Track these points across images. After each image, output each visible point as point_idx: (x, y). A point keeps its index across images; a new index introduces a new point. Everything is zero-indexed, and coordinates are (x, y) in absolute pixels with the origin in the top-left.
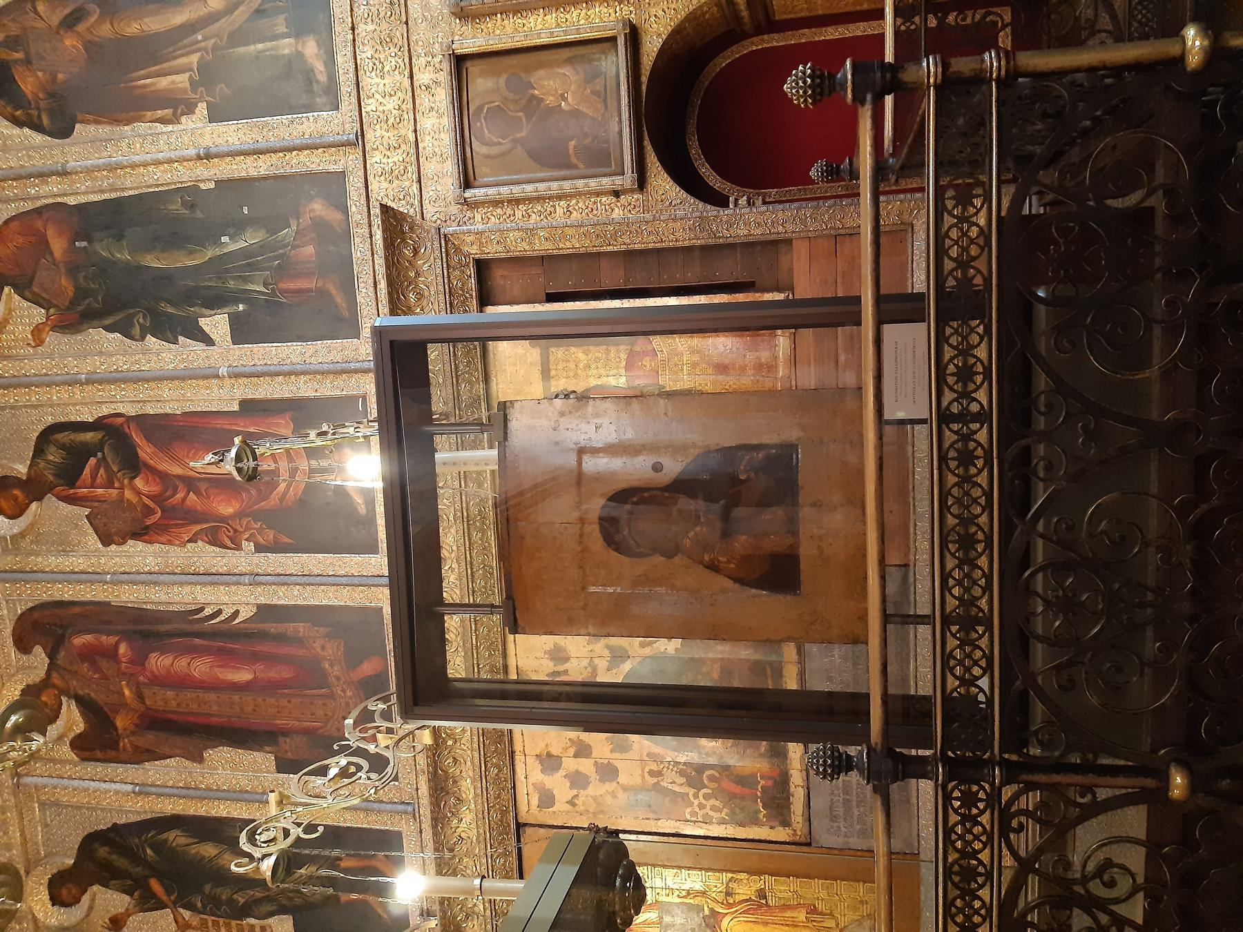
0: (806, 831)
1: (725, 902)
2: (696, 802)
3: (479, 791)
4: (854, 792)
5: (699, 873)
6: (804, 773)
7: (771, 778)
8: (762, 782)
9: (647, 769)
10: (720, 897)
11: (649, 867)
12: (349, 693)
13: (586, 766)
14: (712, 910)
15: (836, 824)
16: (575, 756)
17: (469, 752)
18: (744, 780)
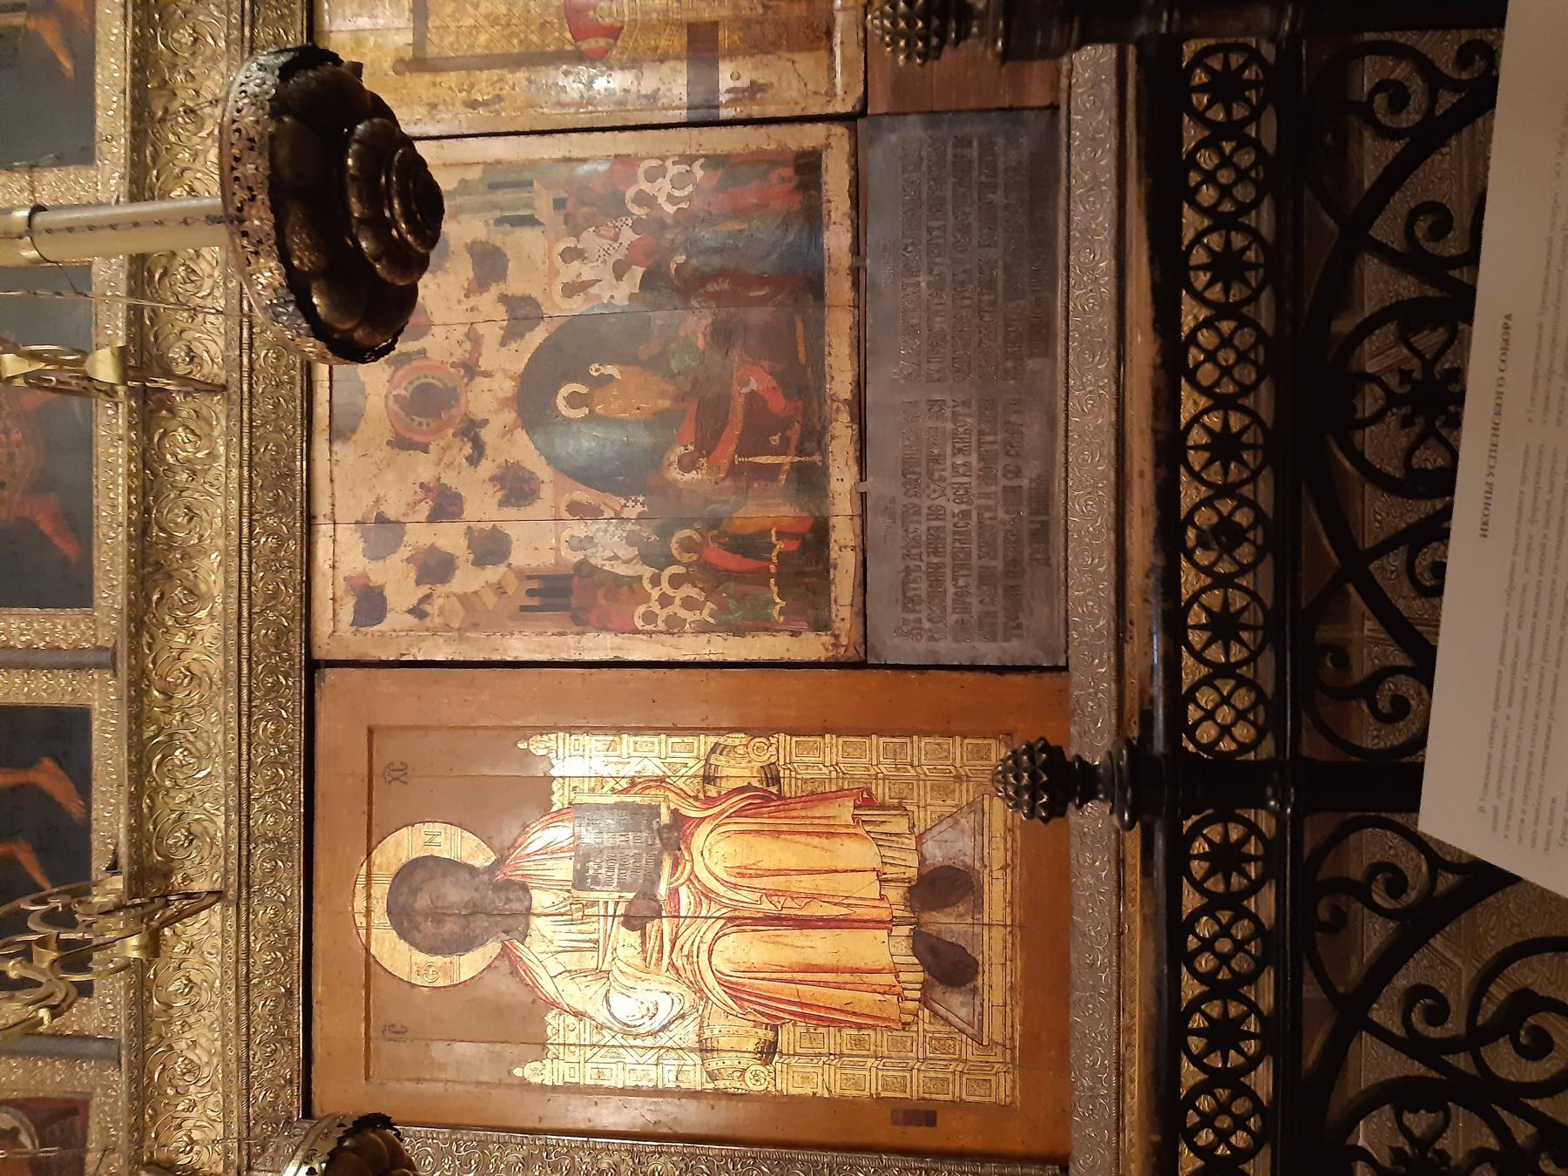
0: (857, 636)
1: (701, 796)
2: (655, 593)
3: (234, 577)
4: (949, 549)
5: (656, 739)
6: (858, 521)
8: (780, 546)
11: (561, 734)
12: (15, 436)
13: (450, 538)
14: (675, 813)
15: (911, 617)
16: (431, 519)
17: (220, 500)
18: (748, 545)
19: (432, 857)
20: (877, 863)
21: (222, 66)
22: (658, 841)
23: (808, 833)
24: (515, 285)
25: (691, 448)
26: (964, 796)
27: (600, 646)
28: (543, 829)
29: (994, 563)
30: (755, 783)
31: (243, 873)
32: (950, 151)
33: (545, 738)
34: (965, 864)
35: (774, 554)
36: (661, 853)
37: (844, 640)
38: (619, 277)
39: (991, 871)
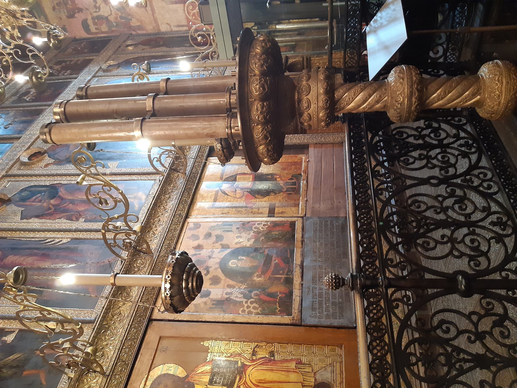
0: (299, 317)
2: (246, 305)
6: (301, 290)
7: (284, 293)
9: (225, 292)
10: (248, 356)
11: (213, 341)
14: (243, 364)
18: (272, 295)
19: (168, 374)
20: (302, 381)
21: (173, 202)
22: (236, 371)
23: (281, 371)
24: (224, 242)
25: (260, 273)
26: (328, 362)
27: (228, 317)
28: (203, 366)
29: (336, 300)
30: (267, 356)
31: (113, 368)
32: (323, 222)
33: (209, 341)
34: (328, 382)
35: (278, 297)
36: (237, 375)
37: (295, 318)
38: (248, 241)
39: (336, 384)
